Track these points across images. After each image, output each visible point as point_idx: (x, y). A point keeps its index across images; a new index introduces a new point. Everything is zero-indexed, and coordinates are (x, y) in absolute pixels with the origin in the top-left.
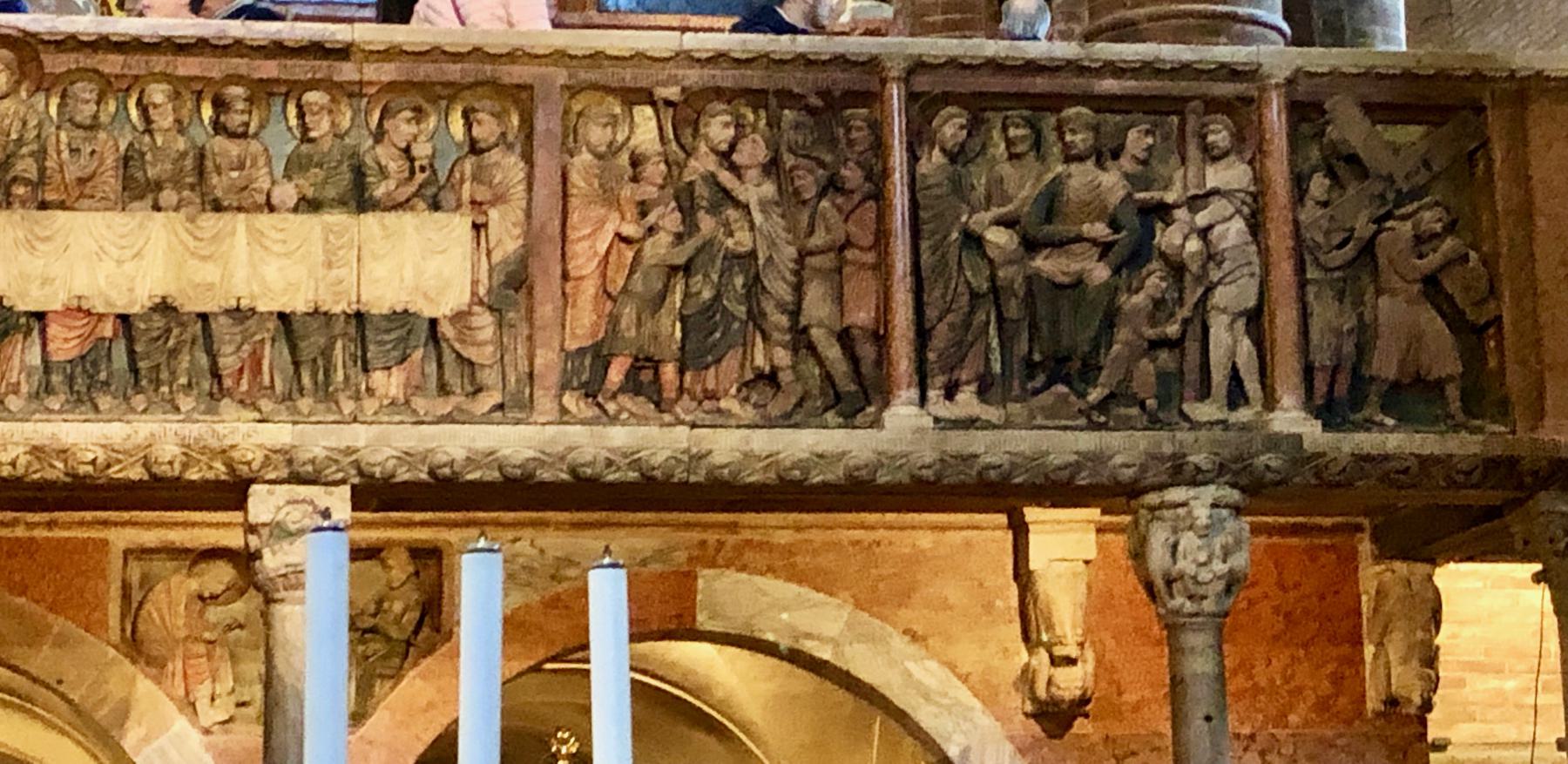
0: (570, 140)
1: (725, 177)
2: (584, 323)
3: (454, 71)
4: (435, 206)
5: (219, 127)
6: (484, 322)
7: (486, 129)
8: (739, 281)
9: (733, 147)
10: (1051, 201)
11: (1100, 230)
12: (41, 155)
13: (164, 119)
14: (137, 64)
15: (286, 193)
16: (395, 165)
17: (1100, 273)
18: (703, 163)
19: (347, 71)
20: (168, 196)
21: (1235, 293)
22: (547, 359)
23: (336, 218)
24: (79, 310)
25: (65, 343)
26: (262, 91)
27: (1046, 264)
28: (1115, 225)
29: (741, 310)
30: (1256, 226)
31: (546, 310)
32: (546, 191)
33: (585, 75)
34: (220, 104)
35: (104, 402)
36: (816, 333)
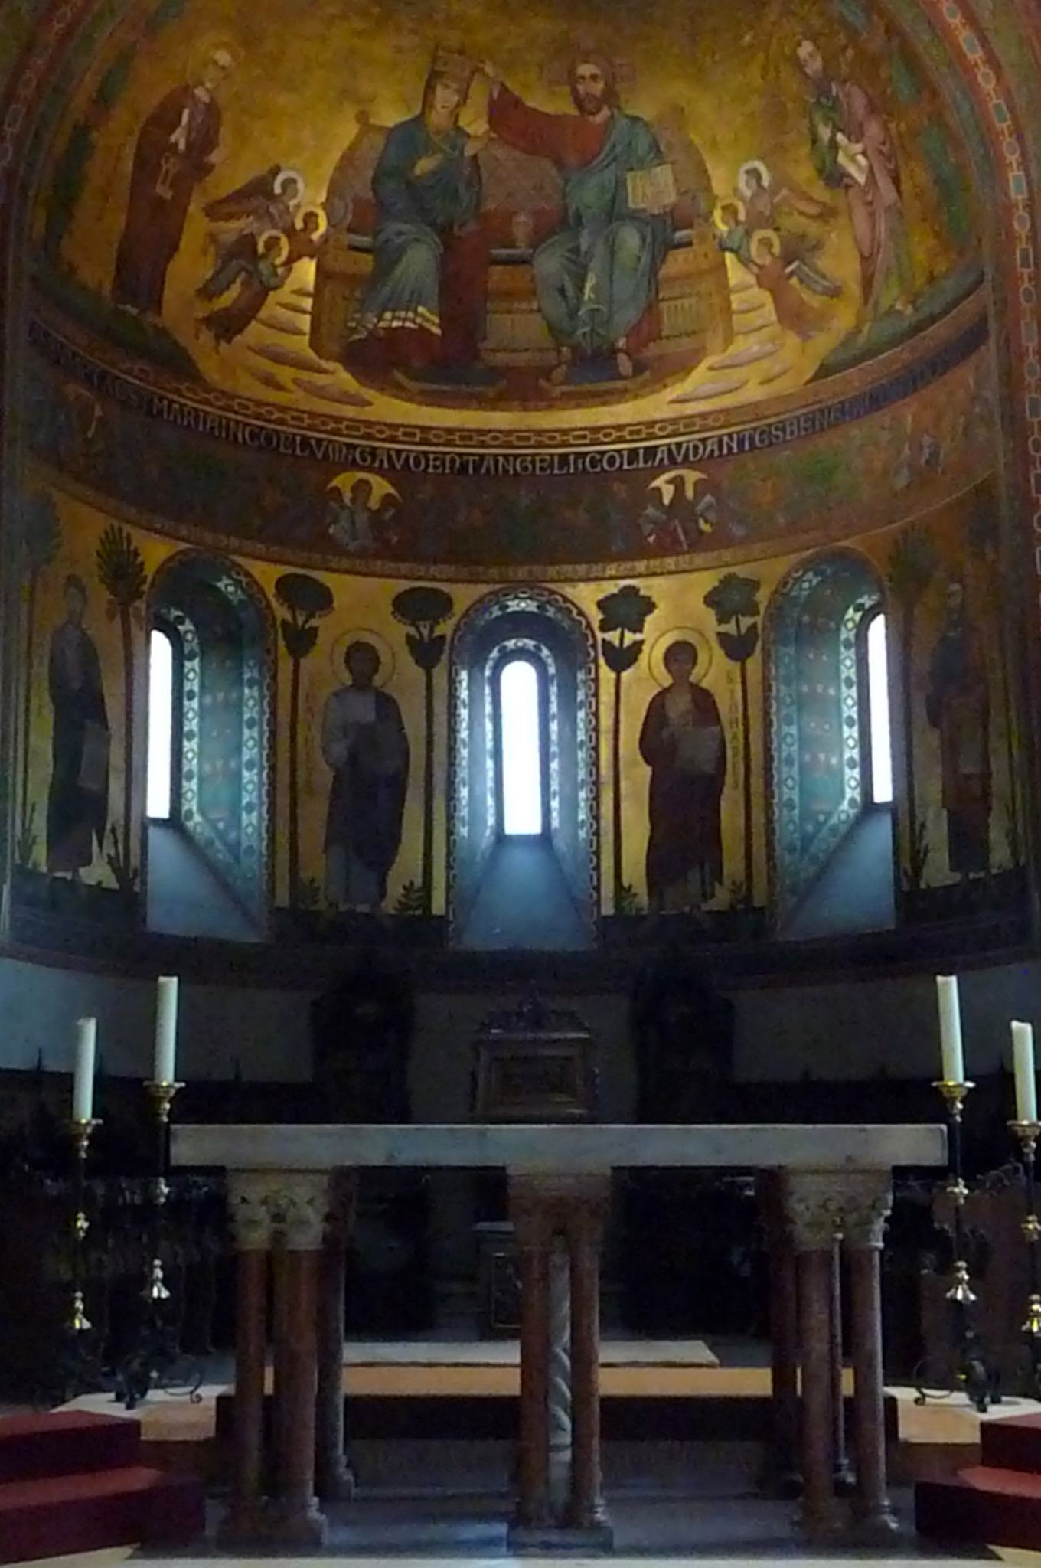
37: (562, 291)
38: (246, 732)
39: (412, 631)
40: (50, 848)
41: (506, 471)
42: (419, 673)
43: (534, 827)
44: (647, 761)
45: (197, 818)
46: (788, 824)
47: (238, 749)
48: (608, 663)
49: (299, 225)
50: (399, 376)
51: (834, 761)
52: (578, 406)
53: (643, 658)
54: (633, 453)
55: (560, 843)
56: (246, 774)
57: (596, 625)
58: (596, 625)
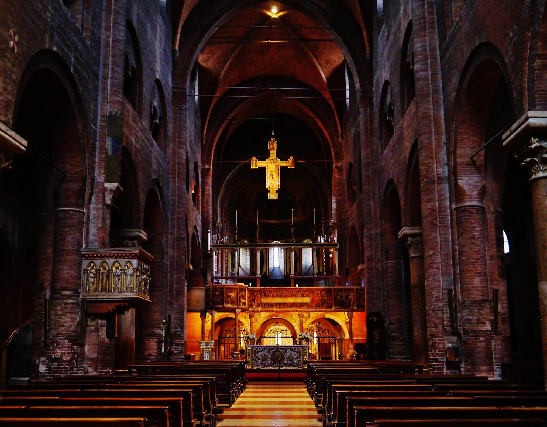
0: (315, 293)
10: (342, 296)
18: (322, 294)
21: (352, 301)
22: (314, 305)
24: (289, 303)
25: (289, 305)
30: (354, 297)
43: (278, 266)
55: (281, 268)
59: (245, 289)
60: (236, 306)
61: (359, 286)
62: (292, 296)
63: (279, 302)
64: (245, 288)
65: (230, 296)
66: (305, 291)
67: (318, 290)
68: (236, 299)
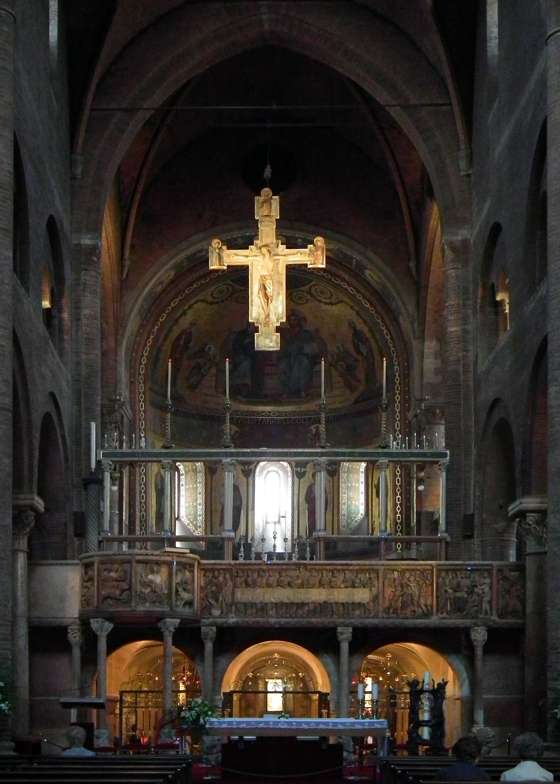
0: (385, 577)
1: (408, 583)
2: (387, 604)
3: (367, 567)
4: (364, 587)
5: (332, 576)
6: (372, 604)
7: (372, 576)
8: (410, 598)
9: (409, 578)
10: (459, 585)
11: (466, 589)
12: (307, 580)
13: (324, 576)
14: (321, 567)
15: (342, 586)
16: (358, 581)
17: (466, 596)
19: (351, 568)
20: (325, 586)
23: (350, 589)
24: (313, 602)
26: (338, 571)
27: (458, 594)
28: (468, 588)
29: (410, 602)
31: (380, 602)
32: (380, 585)
33: (387, 567)
34: (333, 573)
35: (317, 616)
36: (422, 605)
37: (285, 373)
38: (198, 496)
39: (242, 467)
40: (156, 527)
41: (269, 423)
42: (245, 479)
44: (307, 502)
45: (185, 518)
46: (343, 521)
47: (196, 500)
48: (297, 476)
49: (212, 358)
50: (239, 397)
51: (357, 504)
52: (290, 405)
53: (306, 475)
54: (305, 419)
56: (198, 507)
57: (294, 466)
58: (294, 466)
59: (193, 566)
60: (166, 609)
61: (502, 560)
62: (321, 585)
63: (286, 601)
64: (190, 561)
65: (151, 582)
66: (359, 571)
67: (393, 570)
68: (166, 592)
